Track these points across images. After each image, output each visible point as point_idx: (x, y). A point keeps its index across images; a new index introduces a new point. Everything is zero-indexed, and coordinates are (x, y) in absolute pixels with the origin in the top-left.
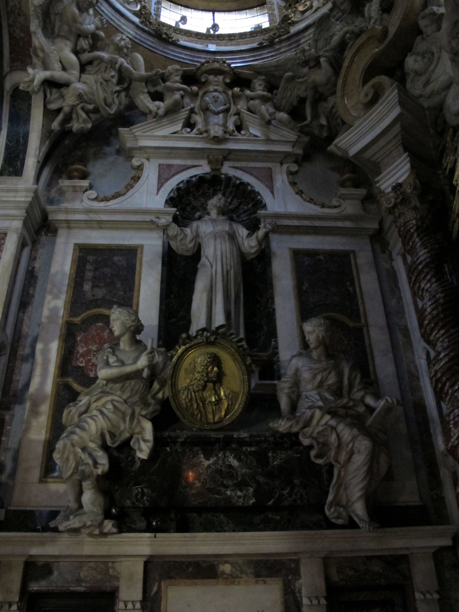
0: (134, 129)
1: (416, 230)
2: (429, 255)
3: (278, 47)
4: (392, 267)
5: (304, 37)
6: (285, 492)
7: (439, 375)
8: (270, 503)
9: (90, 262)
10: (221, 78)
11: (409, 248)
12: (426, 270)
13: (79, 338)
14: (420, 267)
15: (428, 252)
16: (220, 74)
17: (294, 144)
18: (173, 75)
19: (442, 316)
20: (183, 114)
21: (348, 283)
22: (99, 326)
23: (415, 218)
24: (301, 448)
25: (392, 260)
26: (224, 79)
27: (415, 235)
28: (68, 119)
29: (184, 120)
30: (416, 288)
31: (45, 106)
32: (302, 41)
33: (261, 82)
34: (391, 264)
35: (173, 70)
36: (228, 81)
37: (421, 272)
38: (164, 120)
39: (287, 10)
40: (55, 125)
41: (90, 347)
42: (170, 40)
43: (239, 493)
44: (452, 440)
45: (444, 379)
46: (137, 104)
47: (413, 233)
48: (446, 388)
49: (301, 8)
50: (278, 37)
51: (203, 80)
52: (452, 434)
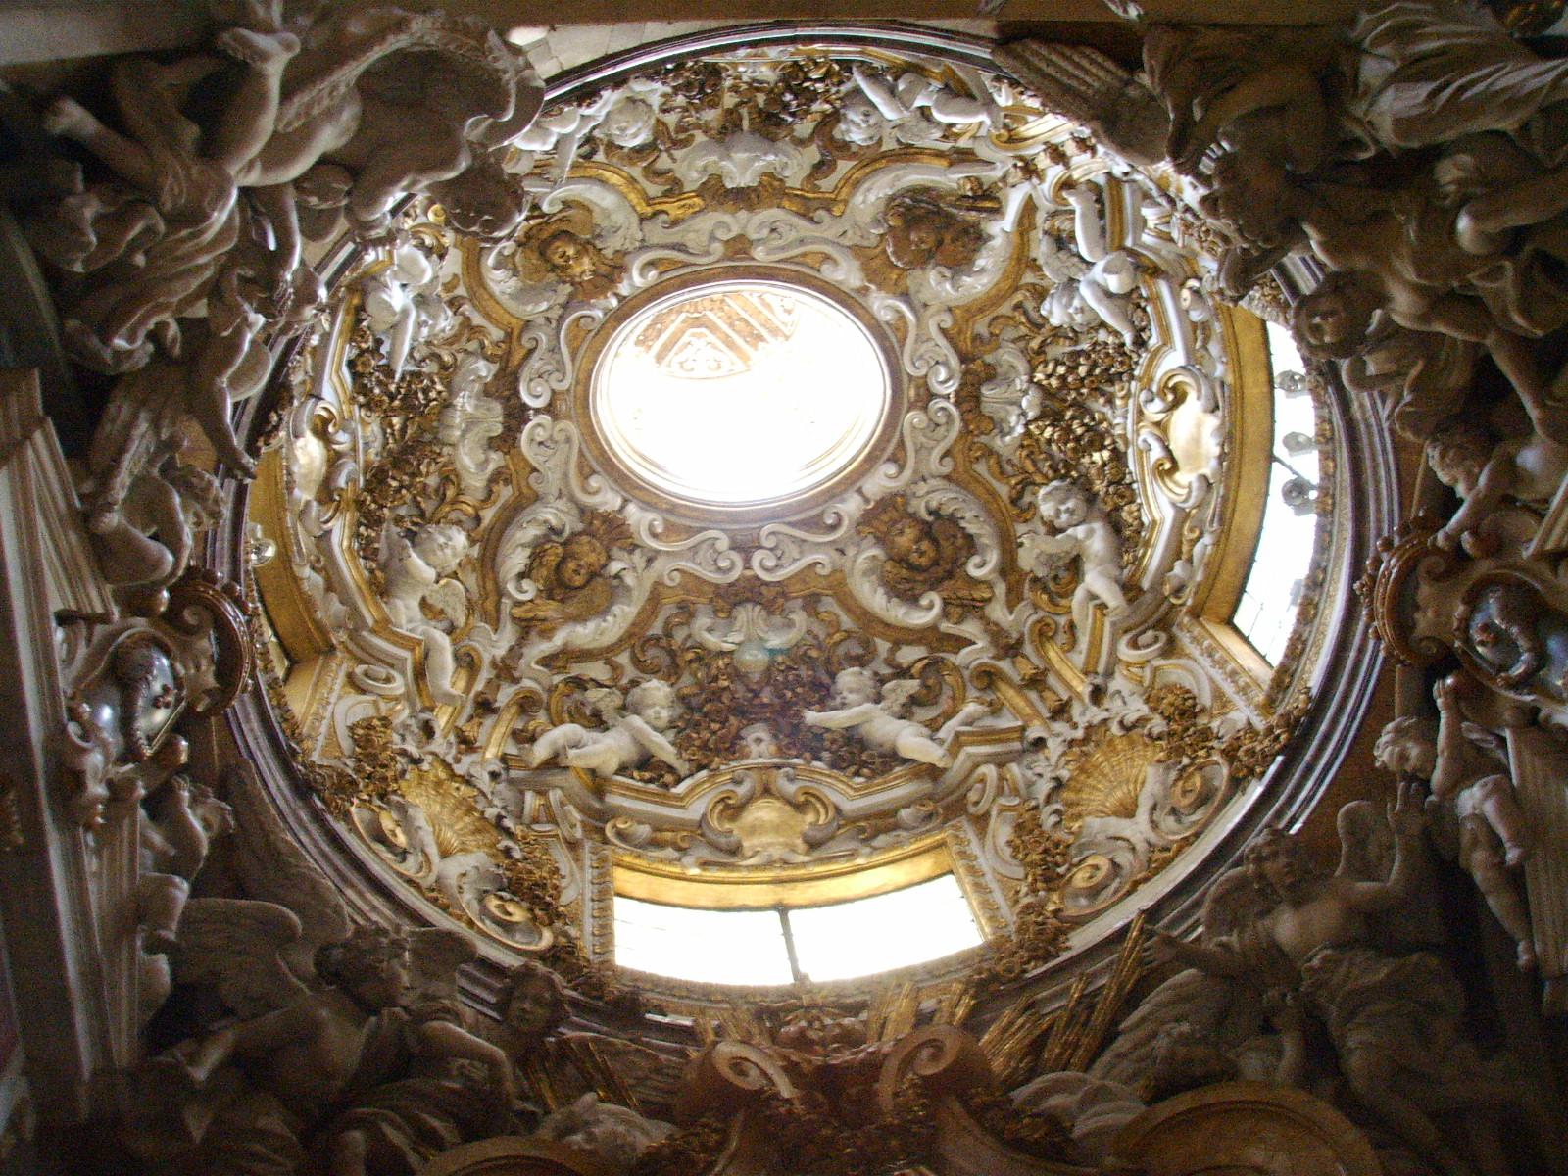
0: (47, 438)
3: (304, 816)
5: (360, 894)
10: (210, 681)
16: (218, 675)
17: (105, 1069)
18: (198, 506)
20: (94, 593)
26: (209, 692)
28: (99, 172)
29: (74, 607)
31: (121, 57)
32: (349, 892)
33: (215, 822)
35: (216, 501)
36: (199, 709)
38: (73, 538)
39: (357, 770)
40: (74, 117)
42: (260, 443)
46: (112, 408)
49: (387, 822)
50: (323, 800)
51: (189, 616)
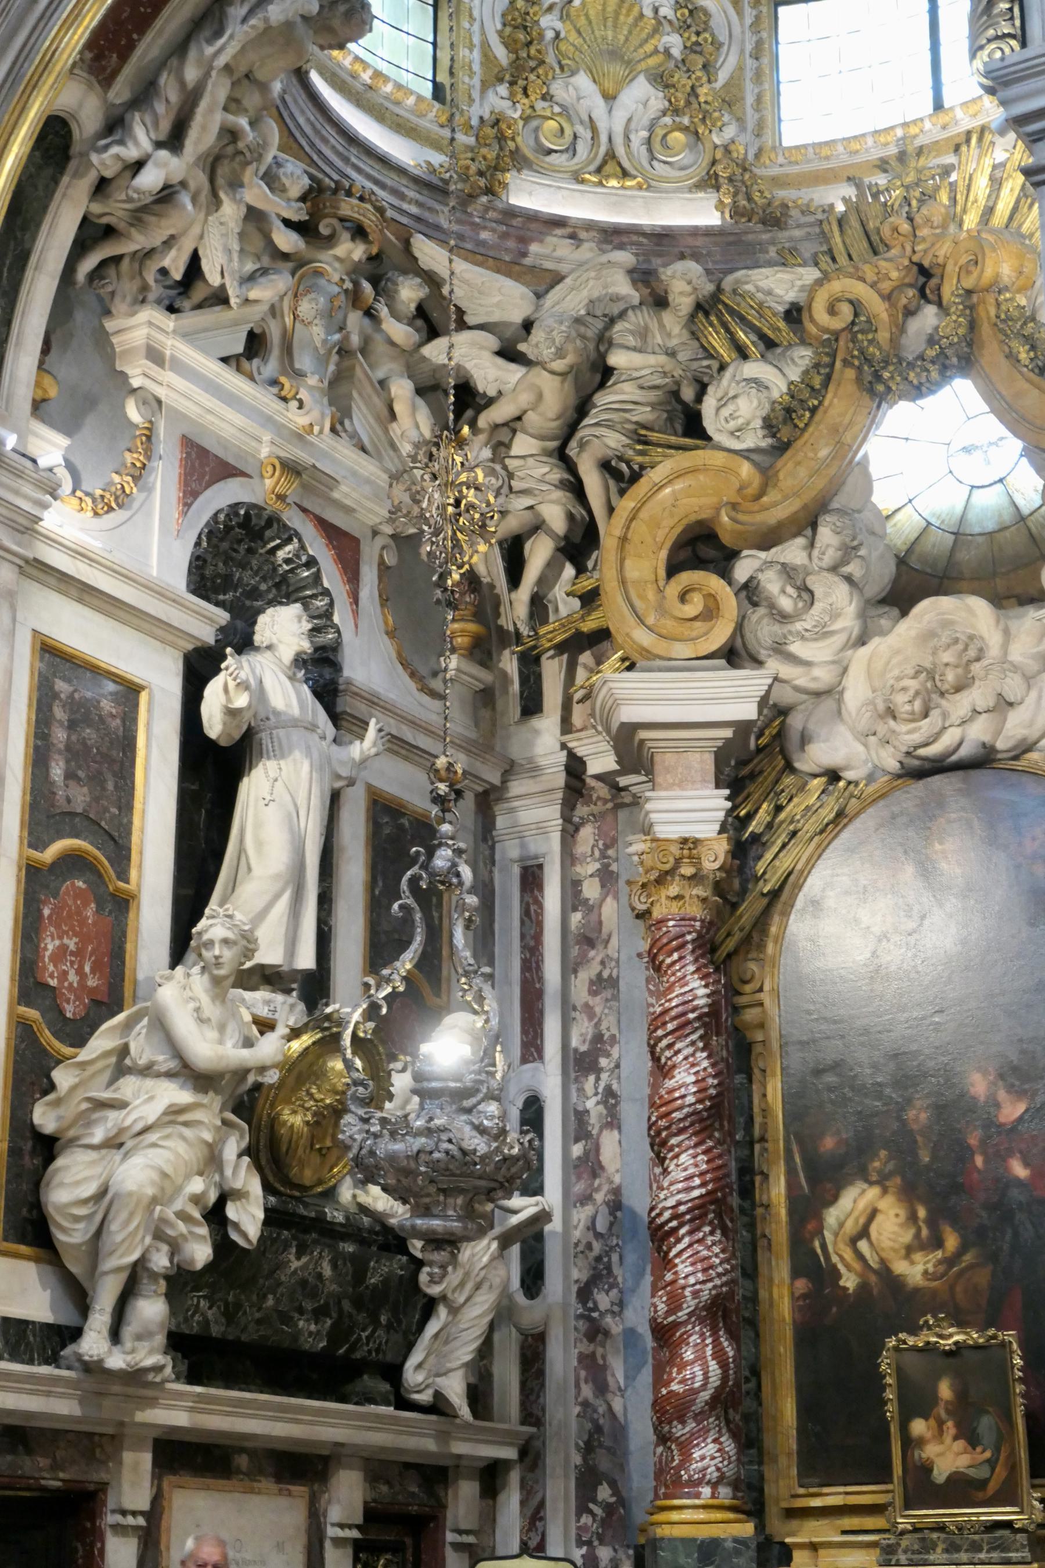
1: (693, 941)
2: (710, 1001)
4: (492, 880)
6: (364, 1335)
7: (682, 1208)
8: (341, 1351)
9: (61, 700)
11: (669, 961)
12: (696, 1025)
13: (46, 912)
14: (691, 1016)
15: (708, 996)
19: (705, 1114)
21: (434, 900)
22: (79, 888)
23: (702, 921)
24: (405, 1258)
25: (493, 863)
27: (690, 947)
30: (664, 1043)
34: (491, 872)
37: (689, 1022)
41: (66, 941)
43: (313, 1327)
44: (680, 1314)
45: (688, 1217)
47: (687, 942)
48: (682, 1231)
52: (685, 1306)
